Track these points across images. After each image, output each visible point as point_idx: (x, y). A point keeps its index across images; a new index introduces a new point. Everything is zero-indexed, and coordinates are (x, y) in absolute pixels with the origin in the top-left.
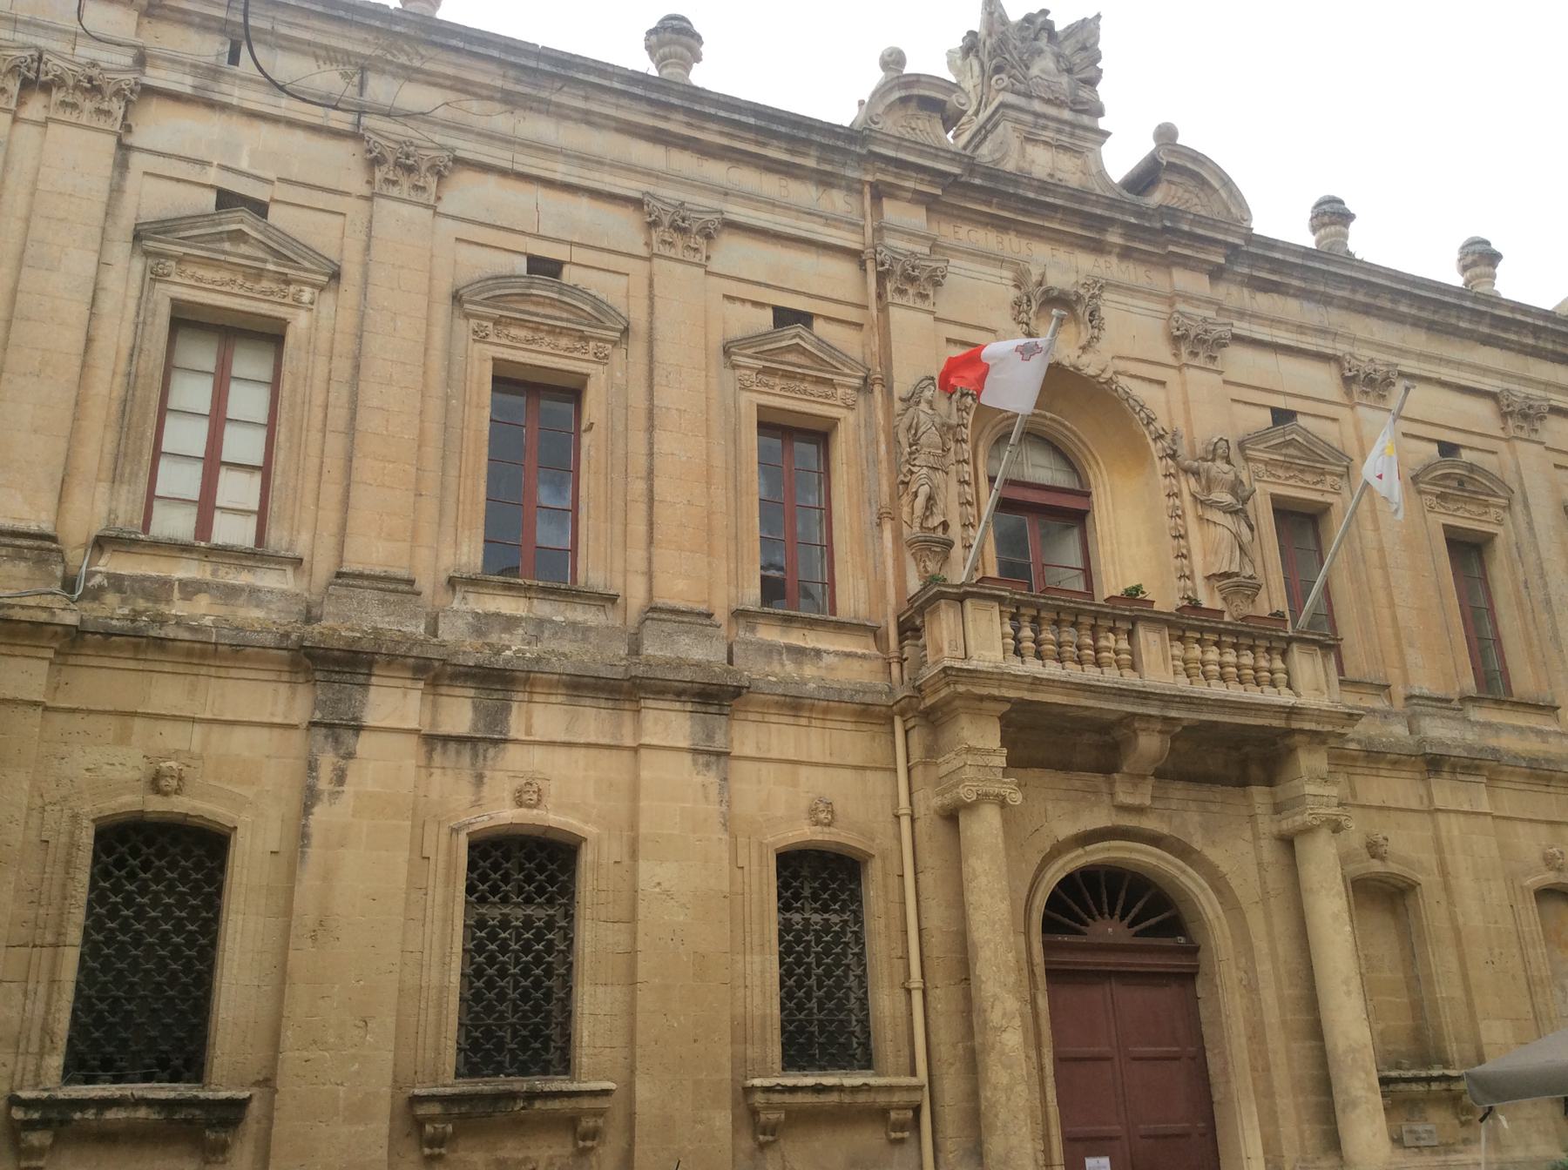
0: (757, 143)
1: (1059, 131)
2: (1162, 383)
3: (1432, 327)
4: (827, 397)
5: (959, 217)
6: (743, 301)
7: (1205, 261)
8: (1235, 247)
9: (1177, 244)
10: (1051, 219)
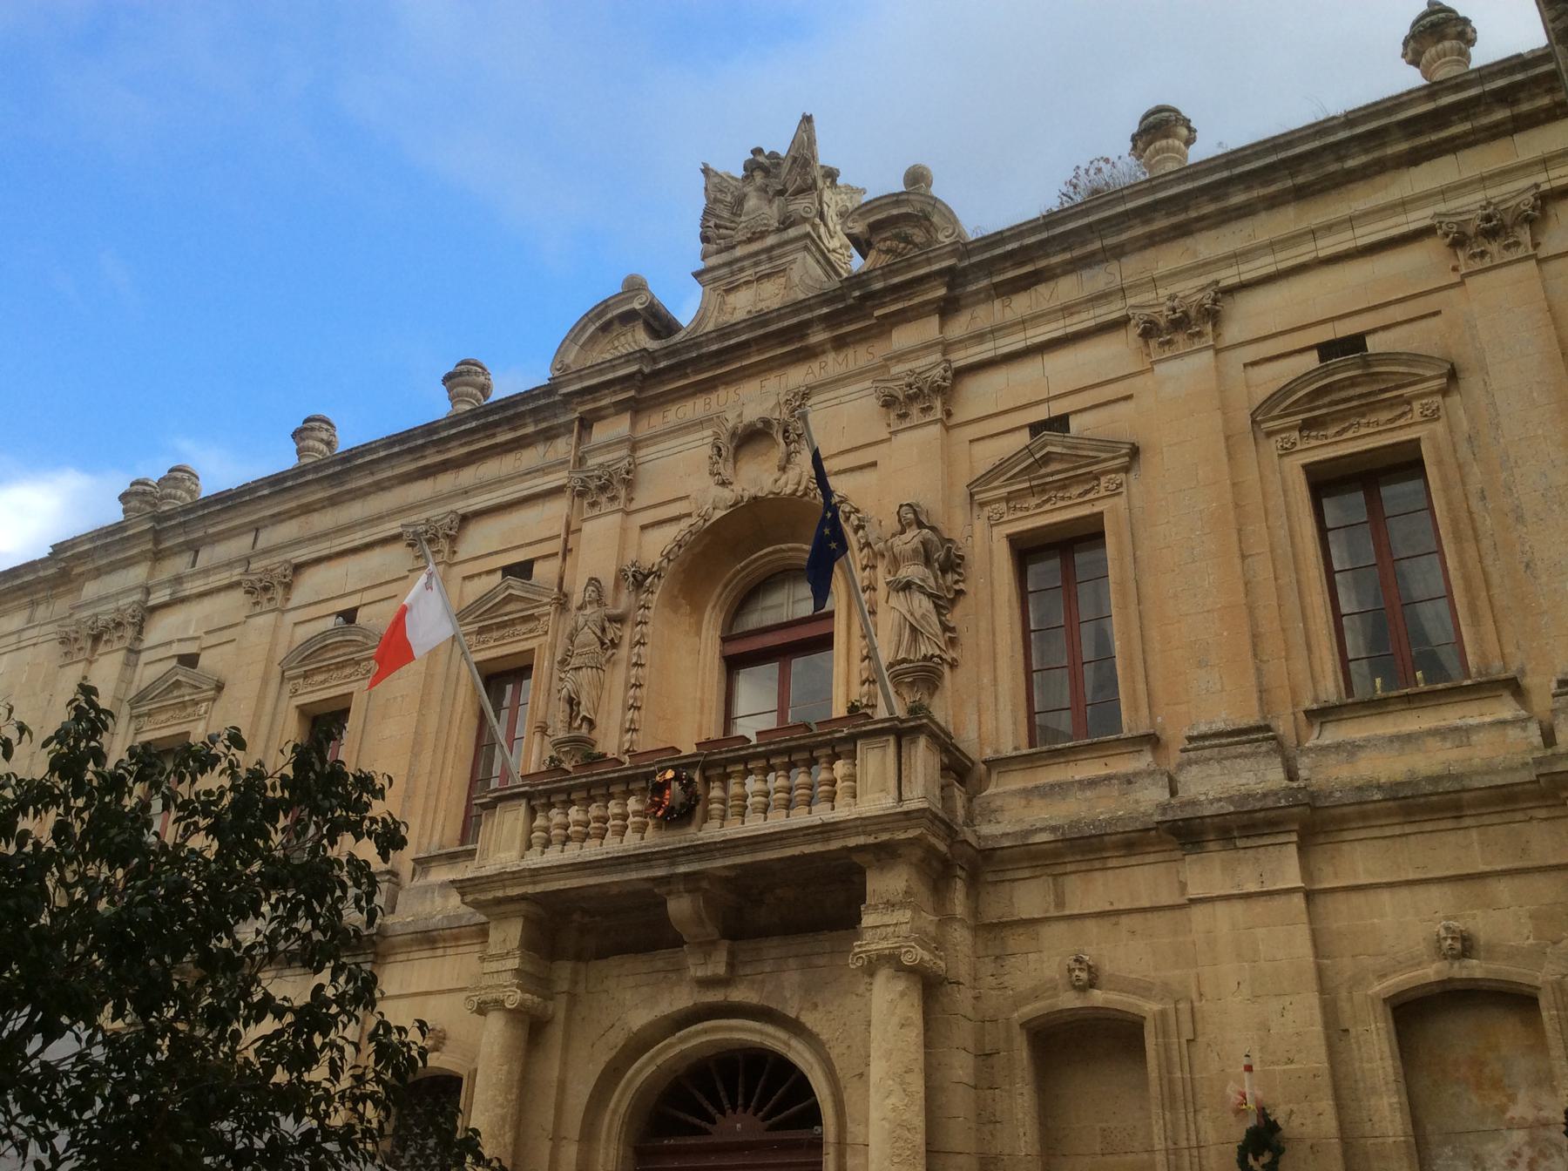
0: (488, 437)
1: (756, 264)
3: (1301, 194)
4: (531, 631)
6: (479, 575)
9: (883, 305)
10: (749, 355)
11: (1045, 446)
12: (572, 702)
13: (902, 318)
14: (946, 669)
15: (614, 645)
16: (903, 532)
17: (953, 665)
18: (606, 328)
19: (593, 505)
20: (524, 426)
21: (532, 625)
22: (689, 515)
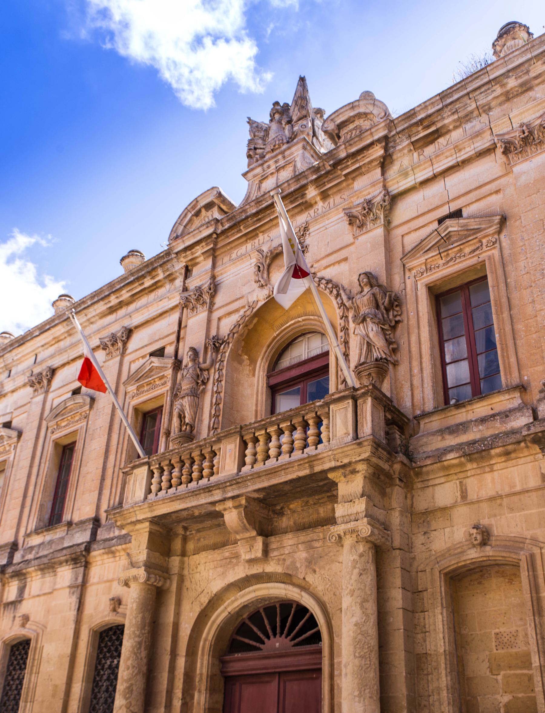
0: (140, 285)
2: (346, 259)
5: (232, 248)
7: (372, 161)
8: (386, 138)
9: (347, 167)
11: (447, 228)
12: (181, 417)
13: (358, 172)
14: (391, 367)
15: (204, 383)
16: (361, 292)
17: (395, 364)
18: (198, 214)
19: (193, 309)
20: (157, 275)
21: (163, 381)
22: (244, 307)
